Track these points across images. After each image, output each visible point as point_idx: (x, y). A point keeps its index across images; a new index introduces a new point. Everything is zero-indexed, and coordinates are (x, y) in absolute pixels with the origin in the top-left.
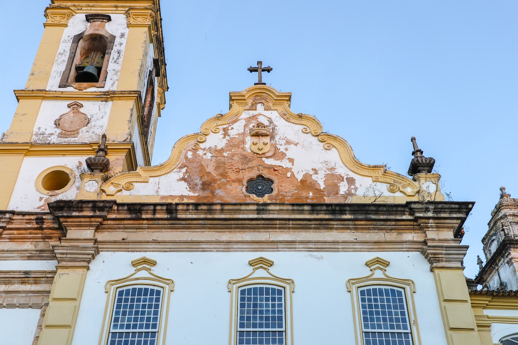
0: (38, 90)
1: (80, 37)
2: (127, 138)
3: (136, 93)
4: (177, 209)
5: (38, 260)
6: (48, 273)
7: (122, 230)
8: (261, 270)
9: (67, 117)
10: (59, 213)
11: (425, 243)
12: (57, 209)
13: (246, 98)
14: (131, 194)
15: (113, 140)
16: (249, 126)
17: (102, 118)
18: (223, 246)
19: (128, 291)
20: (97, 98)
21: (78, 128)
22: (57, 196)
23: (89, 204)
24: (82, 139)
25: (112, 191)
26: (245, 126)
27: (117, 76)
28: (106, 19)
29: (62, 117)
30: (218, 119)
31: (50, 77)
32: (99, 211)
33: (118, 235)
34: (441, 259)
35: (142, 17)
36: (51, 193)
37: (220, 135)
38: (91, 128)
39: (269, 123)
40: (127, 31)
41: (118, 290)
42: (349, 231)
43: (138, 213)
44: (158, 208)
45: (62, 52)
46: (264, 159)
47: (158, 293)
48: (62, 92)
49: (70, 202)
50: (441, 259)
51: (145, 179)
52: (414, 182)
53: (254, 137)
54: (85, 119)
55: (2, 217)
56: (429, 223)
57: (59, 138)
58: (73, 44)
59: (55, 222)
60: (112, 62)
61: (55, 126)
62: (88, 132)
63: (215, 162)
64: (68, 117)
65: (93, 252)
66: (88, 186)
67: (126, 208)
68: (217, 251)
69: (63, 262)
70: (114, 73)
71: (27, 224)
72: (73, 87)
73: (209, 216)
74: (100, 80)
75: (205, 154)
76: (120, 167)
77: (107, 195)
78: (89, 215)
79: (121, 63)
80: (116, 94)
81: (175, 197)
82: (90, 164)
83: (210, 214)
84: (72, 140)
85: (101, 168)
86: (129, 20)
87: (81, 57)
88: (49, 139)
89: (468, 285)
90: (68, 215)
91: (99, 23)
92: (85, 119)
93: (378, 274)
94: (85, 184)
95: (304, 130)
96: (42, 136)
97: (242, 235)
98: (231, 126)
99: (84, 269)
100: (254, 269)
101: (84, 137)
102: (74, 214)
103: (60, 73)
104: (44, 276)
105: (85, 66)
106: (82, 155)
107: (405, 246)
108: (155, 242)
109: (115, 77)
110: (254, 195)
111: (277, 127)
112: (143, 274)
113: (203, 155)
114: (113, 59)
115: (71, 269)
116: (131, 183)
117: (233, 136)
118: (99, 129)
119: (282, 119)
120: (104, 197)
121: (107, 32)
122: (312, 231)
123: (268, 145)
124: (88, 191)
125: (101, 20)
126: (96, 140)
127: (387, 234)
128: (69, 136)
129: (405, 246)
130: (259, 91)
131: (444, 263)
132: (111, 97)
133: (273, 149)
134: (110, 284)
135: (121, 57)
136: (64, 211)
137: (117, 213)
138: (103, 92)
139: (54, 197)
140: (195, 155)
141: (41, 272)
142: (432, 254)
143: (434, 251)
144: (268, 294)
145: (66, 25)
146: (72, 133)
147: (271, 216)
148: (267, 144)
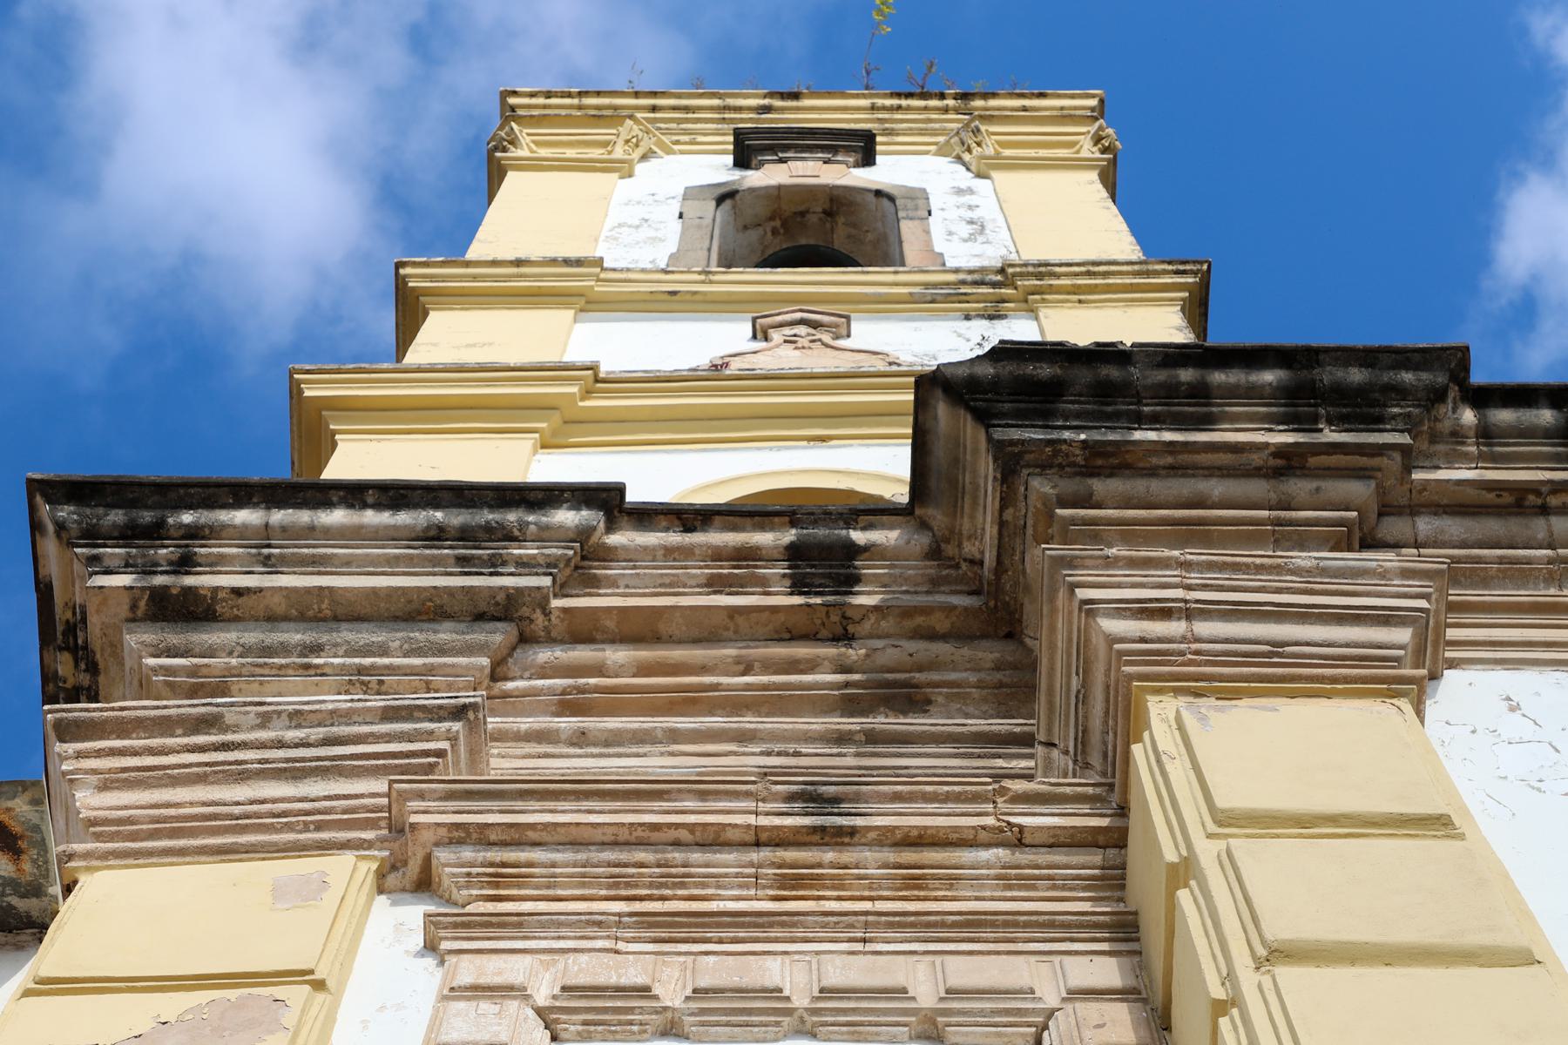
3: (1181, 267)
32: (1342, 421)
55: (523, 525)
59: (945, 572)
71: (715, 593)
80: (1058, 276)
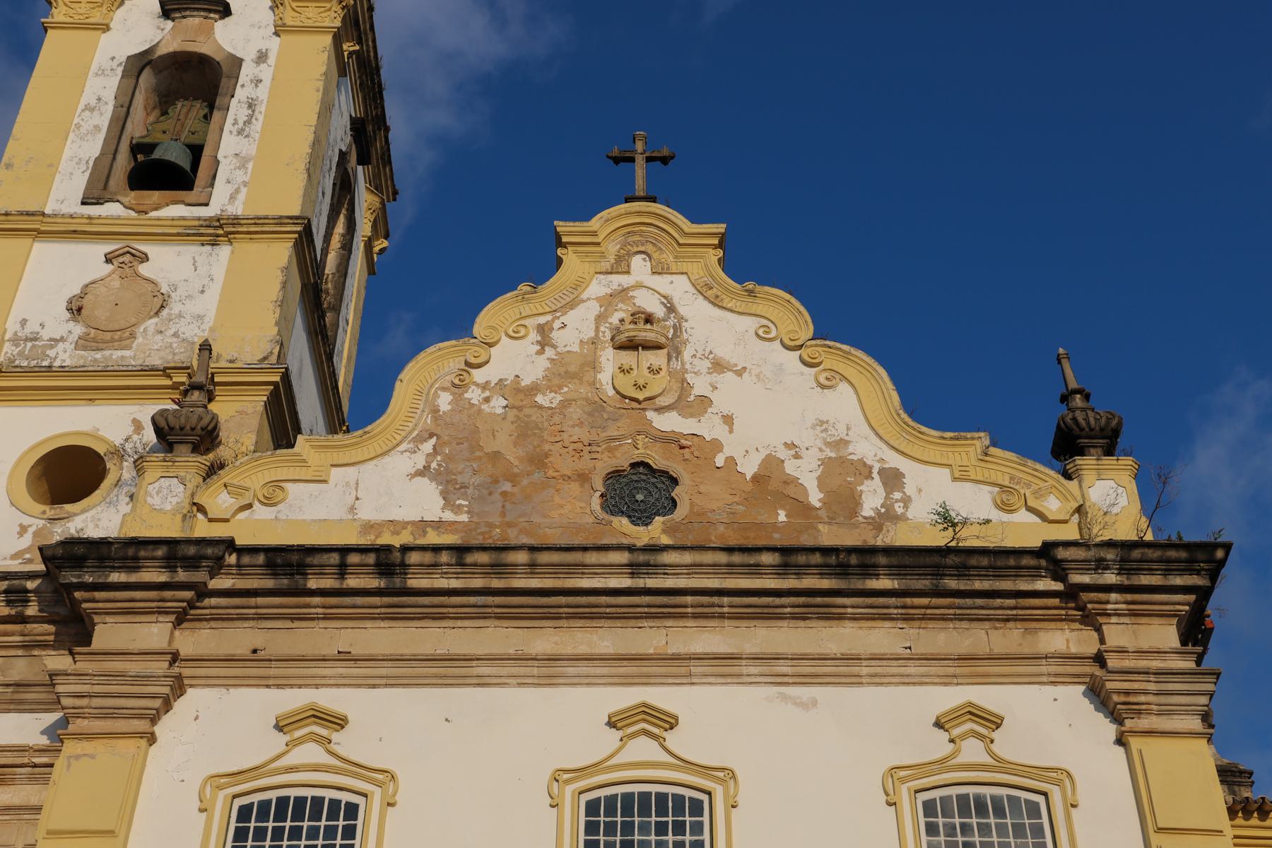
0: (21, 213)
1: (144, 62)
2: (271, 353)
3: (296, 221)
4: (407, 562)
5: (9, 711)
6: (35, 751)
7: (251, 623)
8: (643, 740)
9: (103, 290)
10: (72, 576)
11: (1099, 659)
12: (66, 565)
13: (599, 241)
14: (281, 516)
15: (229, 358)
16: (610, 320)
17: (203, 292)
18: (535, 671)
19: (265, 805)
20: (188, 235)
21: (134, 320)
22: (68, 522)
23: (158, 548)
24: (144, 353)
25: (224, 506)
26: (600, 319)
27: (246, 173)
28: (215, 12)
29: (88, 289)
30: (523, 298)
31: (57, 175)
33: (239, 638)
34: (1144, 707)
35: (316, 7)
36: (53, 512)
37: (529, 345)
38: (170, 320)
39: (665, 309)
40: (274, 44)
41: (238, 802)
42: (888, 624)
43: (297, 574)
44: (353, 558)
45: (93, 102)
46: (650, 415)
47: (352, 810)
48: (90, 218)
49: (104, 543)
50: (1144, 707)
51: (318, 474)
52: (1065, 482)
53: (623, 353)
54: (154, 296)
56: (1108, 602)
57: (77, 352)
58: (124, 80)
60: (231, 132)
61: (68, 315)
62: (161, 332)
63: (516, 422)
64: (106, 289)
65: (166, 690)
66: (158, 493)
67: (261, 559)
68: (520, 685)
69: (80, 720)
70: (238, 165)
72: (122, 203)
73: (496, 583)
74: (197, 183)
75: (487, 400)
76: (249, 435)
77: (211, 520)
78: (157, 581)
79: (257, 136)
81: (405, 525)
82: (163, 428)
83: (499, 575)
84: (116, 356)
85: (196, 440)
86: (281, 15)
87: (147, 114)
88: (52, 353)
89: (1222, 782)
90: (96, 581)
91: (197, 20)
92: (154, 296)
93: (972, 751)
94: (149, 486)
95: (761, 332)
96: (29, 345)
97: (589, 635)
98: (558, 318)
99: (140, 740)
100: (625, 739)
101: (150, 349)
102: (115, 577)
103: (87, 162)
104: (26, 761)
105: (156, 141)
106: (142, 402)
107: (1044, 669)
108: (344, 657)
109: (240, 176)
110: (625, 521)
111: (686, 321)
112: (311, 753)
113: (481, 404)
114: (234, 124)
115: (101, 740)
116: (277, 484)
117: (565, 346)
118: (191, 326)
119: (701, 297)
120: (202, 529)
121: (221, 48)
122: (785, 623)
123: (662, 373)
124: (157, 507)
125: (202, 13)
126: (182, 357)
127: (996, 632)
128: (107, 345)
129: (1044, 669)
130: (638, 220)
131: (1154, 718)
132: (227, 234)
133: (676, 386)
134: (214, 784)
135: (256, 119)
136: (86, 570)
137: (238, 574)
138: (205, 220)
139: (59, 525)
140: (458, 399)
141: (17, 751)
142: (1119, 692)
143: (1126, 683)
144: (662, 811)
145: (106, 28)
146: (116, 337)
147: (670, 583)
148: (658, 373)
